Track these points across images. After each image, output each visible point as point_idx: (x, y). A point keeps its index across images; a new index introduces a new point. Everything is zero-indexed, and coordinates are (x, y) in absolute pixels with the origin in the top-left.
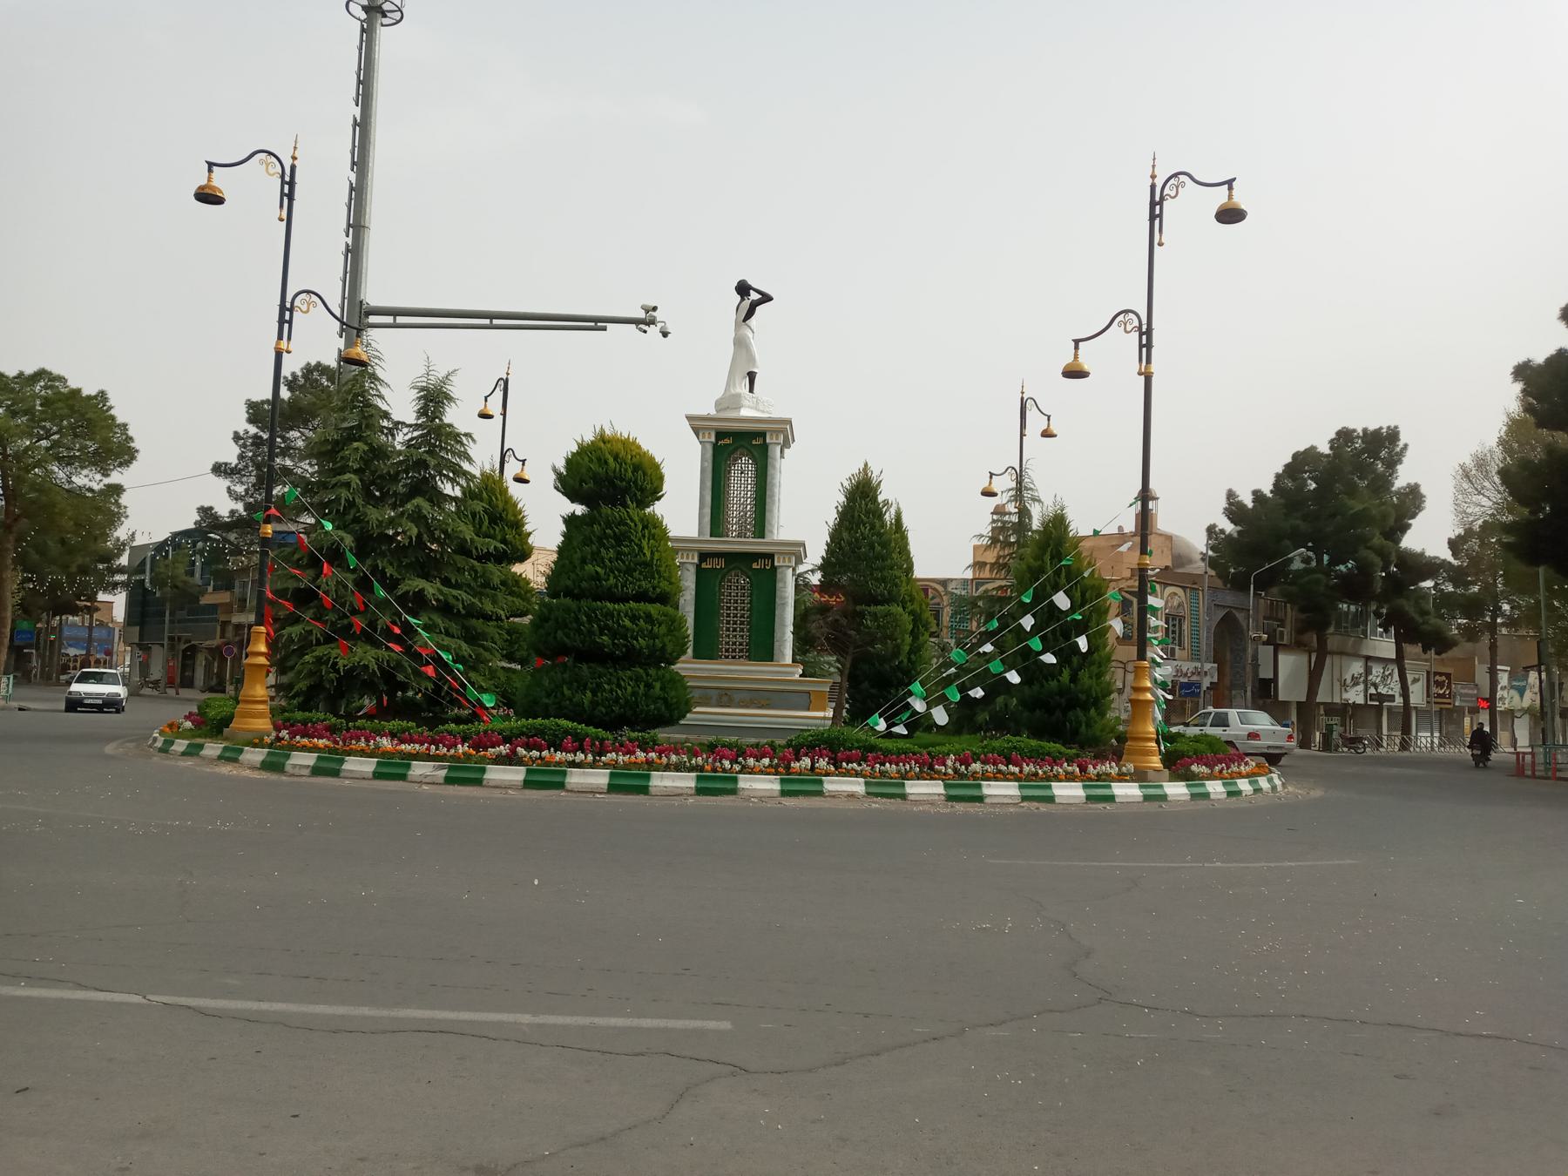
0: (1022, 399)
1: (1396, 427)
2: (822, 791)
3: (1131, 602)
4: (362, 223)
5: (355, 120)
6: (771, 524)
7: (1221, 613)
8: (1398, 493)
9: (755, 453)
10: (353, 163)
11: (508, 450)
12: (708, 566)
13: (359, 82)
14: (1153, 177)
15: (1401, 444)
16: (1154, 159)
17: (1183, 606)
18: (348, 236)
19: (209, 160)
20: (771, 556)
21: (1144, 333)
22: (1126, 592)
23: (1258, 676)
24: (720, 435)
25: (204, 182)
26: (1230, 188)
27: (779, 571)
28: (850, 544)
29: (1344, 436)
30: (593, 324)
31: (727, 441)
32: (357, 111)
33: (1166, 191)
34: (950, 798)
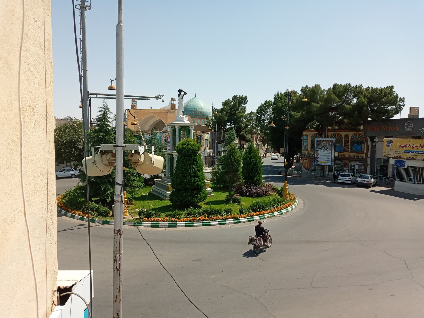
1: (247, 96)
3: (199, 137)
4: (86, 70)
5: (80, 39)
9: (187, 130)
16: (289, 87)
19: (112, 79)
22: (198, 135)
23: (217, 150)
24: (180, 126)
25: (110, 85)
29: (235, 97)
30: (147, 98)
31: (181, 128)
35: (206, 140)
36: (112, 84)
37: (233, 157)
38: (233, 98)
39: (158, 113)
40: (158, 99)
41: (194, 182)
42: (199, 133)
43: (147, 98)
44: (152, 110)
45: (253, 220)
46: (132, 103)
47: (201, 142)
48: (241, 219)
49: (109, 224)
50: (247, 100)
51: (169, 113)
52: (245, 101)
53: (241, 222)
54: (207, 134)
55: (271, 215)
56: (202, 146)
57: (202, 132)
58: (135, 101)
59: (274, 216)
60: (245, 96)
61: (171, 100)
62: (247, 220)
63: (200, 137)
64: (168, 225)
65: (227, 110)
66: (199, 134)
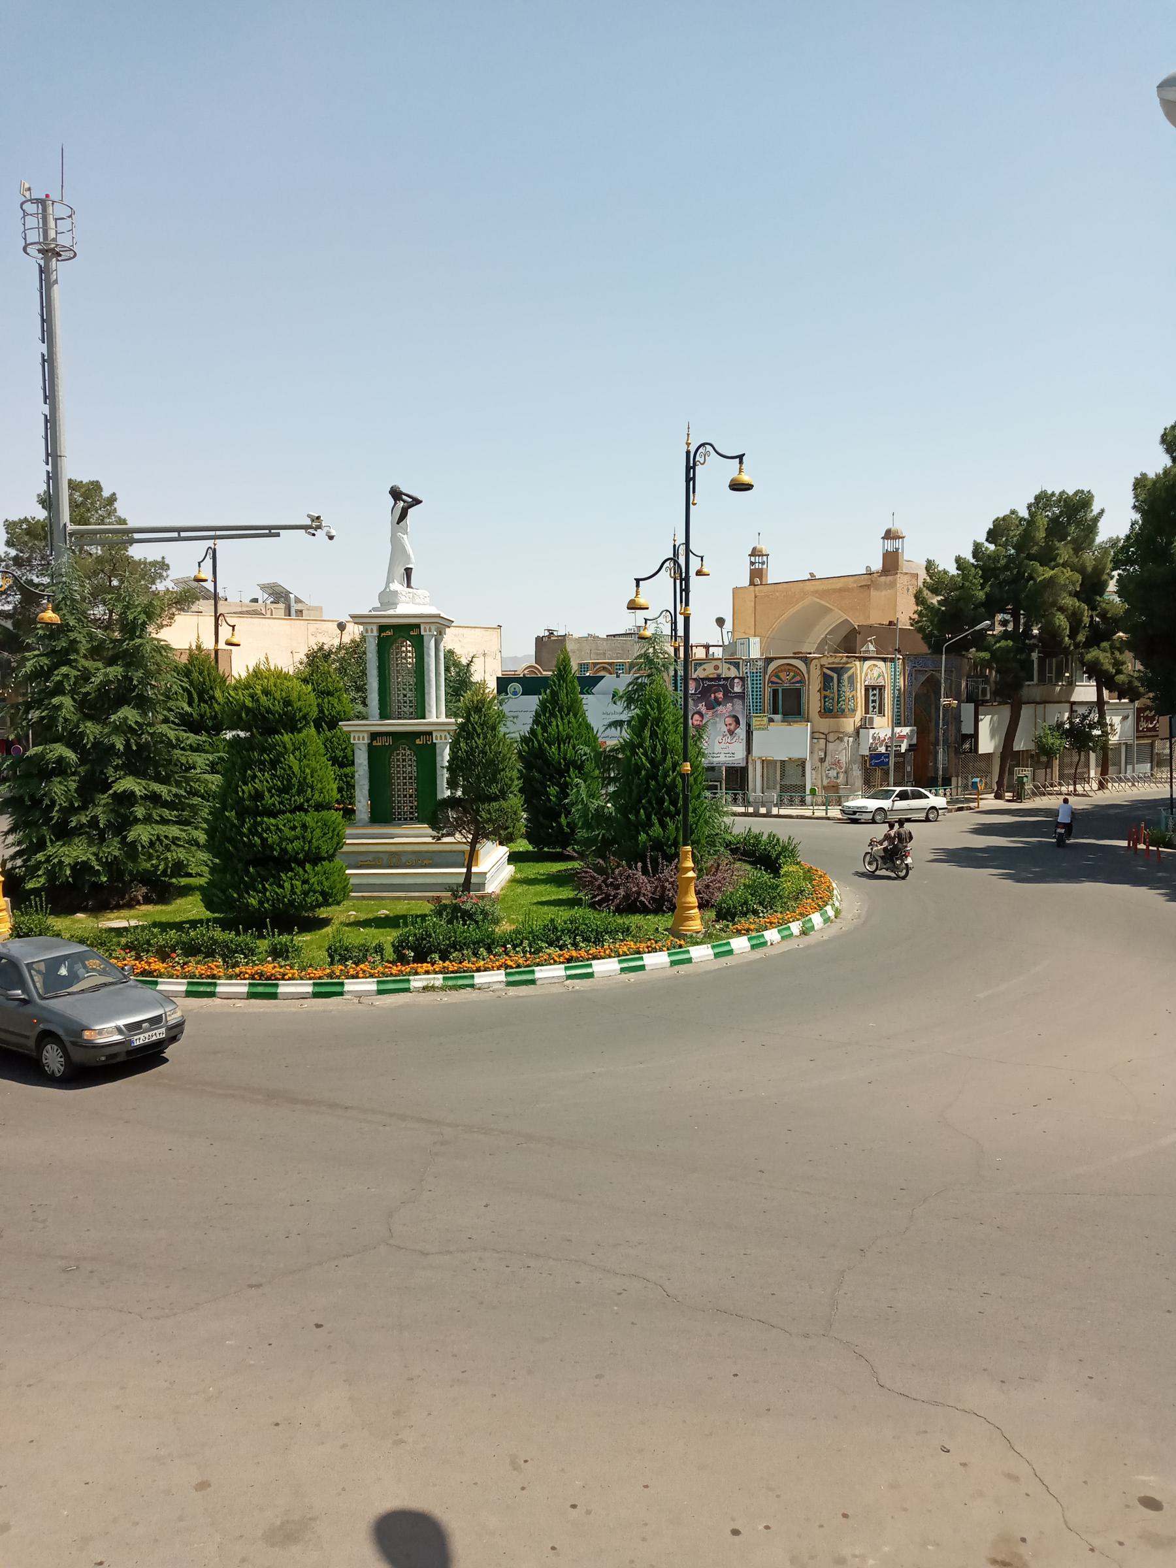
0: (675, 546)
1: (1089, 492)
2: (409, 988)
3: (832, 678)
4: (59, 454)
5: (43, 355)
6: (429, 705)
7: (923, 678)
8: (1100, 547)
10: (46, 397)
11: (220, 614)
12: (378, 744)
13: (43, 321)
14: (688, 444)
15: (1096, 508)
17: (884, 677)
18: (47, 464)
20: (430, 733)
21: (683, 579)
22: (827, 668)
24: (382, 628)
26: (741, 462)
27: (437, 746)
28: (465, 751)
29: (1042, 500)
30: (267, 531)
31: (389, 633)
32: (44, 348)
33: (698, 458)
34: (509, 984)
37: (466, 739)
39: (835, 591)
40: (312, 531)
41: (253, 831)
42: (831, 660)
43: (267, 531)
44: (813, 583)
45: (341, 994)
47: (839, 696)
48: (284, 985)
51: (872, 589)
53: (279, 995)
54: (881, 664)
55: (450, 983)
57: (847, 657)
58: (763, 555)
59: (472, 986)
61: (887, 539)
62: (310, 989)
63: (835, 676)
65: (989, 556)
66: (833, 663)
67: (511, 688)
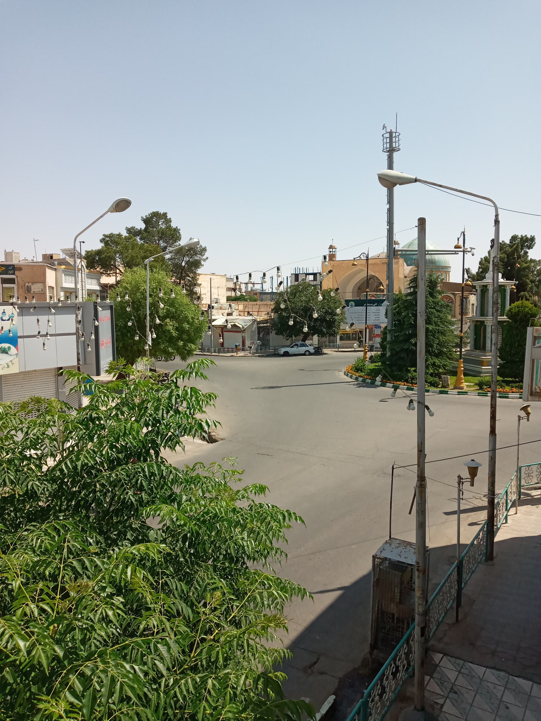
1: (534, 236)
25: (456, 244)
35: (473, 305)
36: (458, 243)
38: (510, 240)
44: (361, 261)
46: (330, 252)
49: (447, 394)
50: (534, 243)
52: (531, 244)
56: (467, 313)
60: (531, 236)
64: (519, 396)
67: (350, 304)
